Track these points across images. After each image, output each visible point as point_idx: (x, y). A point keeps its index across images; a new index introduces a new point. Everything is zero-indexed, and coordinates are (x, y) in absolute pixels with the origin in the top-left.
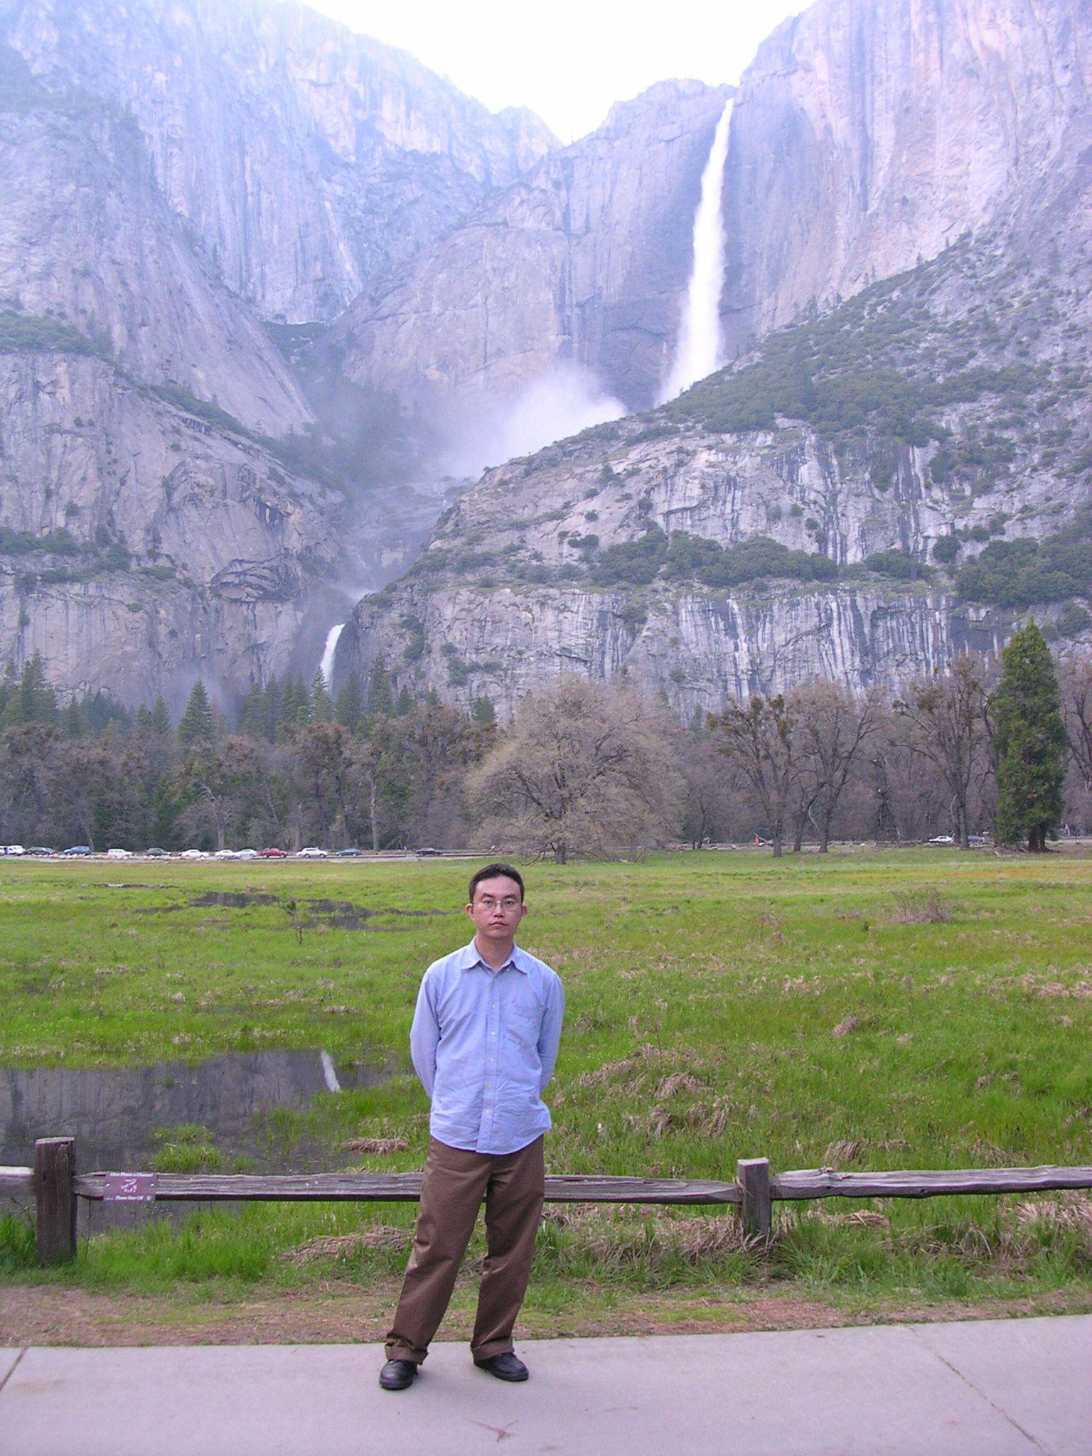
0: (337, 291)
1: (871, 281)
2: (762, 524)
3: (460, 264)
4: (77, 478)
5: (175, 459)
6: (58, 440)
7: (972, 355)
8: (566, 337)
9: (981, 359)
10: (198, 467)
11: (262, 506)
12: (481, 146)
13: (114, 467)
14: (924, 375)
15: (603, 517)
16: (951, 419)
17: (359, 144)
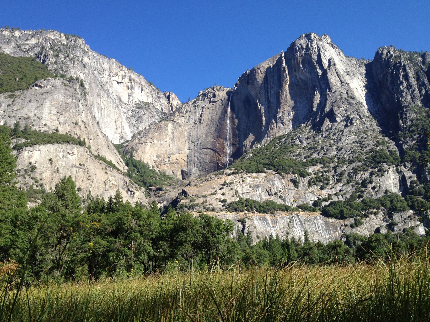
0: (125, 136)
1: (275, 137)
2: (268, 197)
3: (162, 131)
4: (81, 180)
5: (106, 176)
6: (74, 169)
7: (311, 155)
8: (190, 150)
9: (315, 155)
10: (112, 179)
11: (128, 190)
12: (160, 101)
13: (90, 178)
14: (300, 159)
15: (226, 194)
16: (311, 169)
17: (129, 99)
